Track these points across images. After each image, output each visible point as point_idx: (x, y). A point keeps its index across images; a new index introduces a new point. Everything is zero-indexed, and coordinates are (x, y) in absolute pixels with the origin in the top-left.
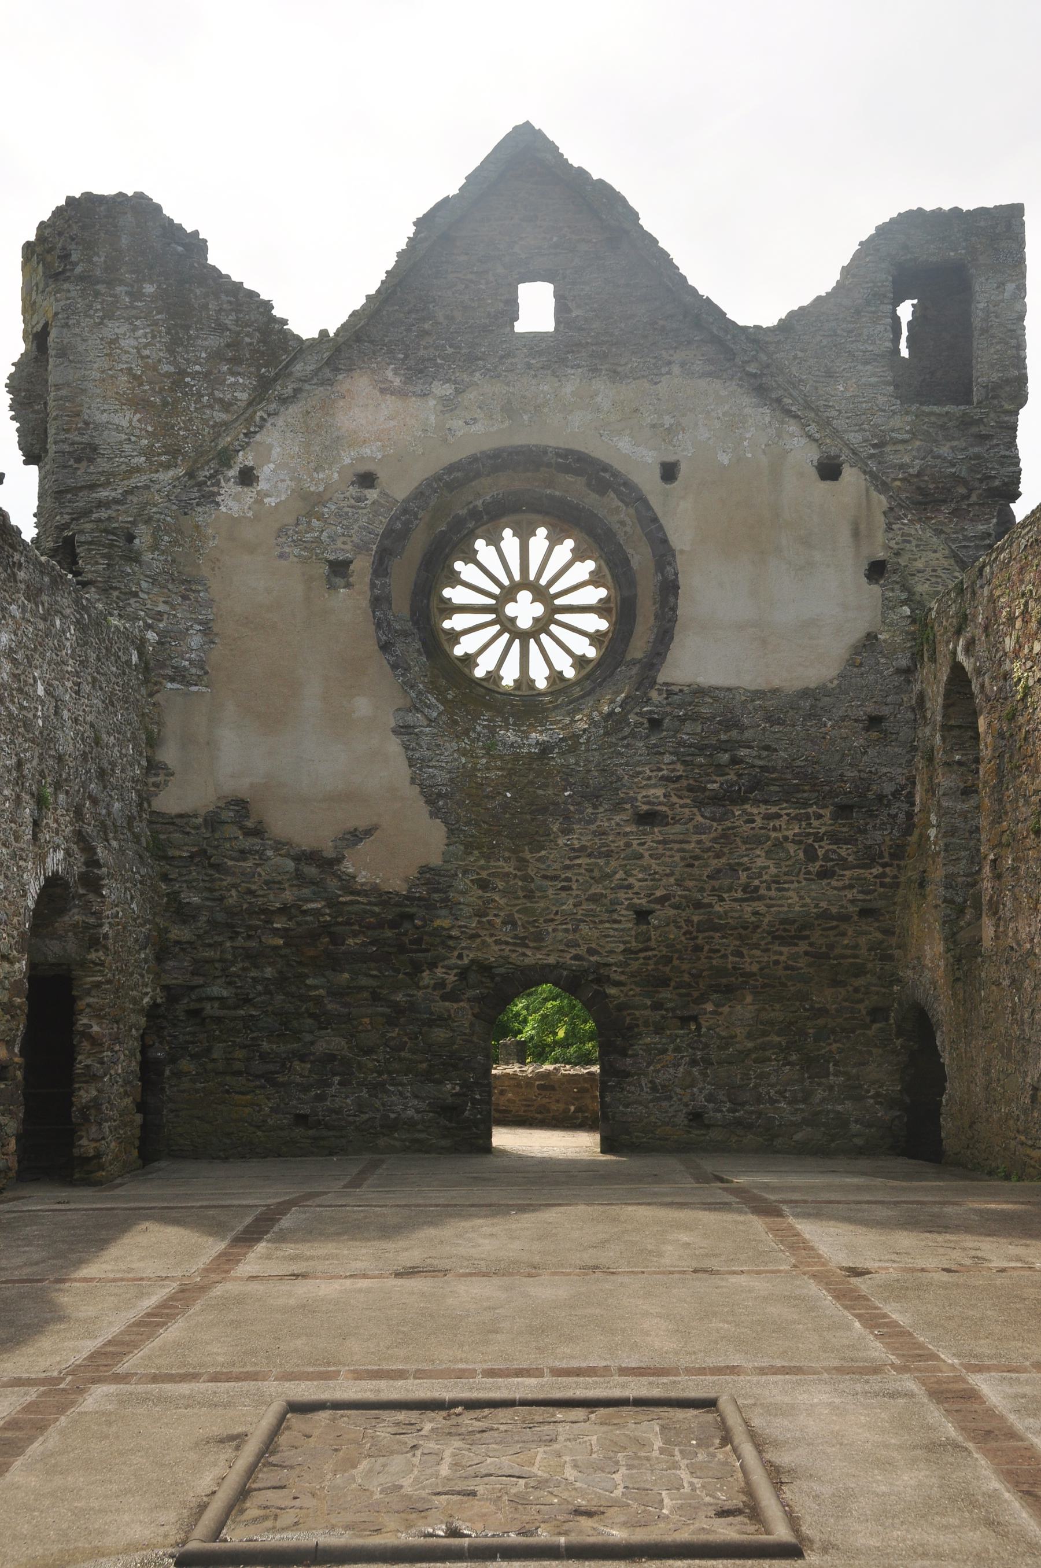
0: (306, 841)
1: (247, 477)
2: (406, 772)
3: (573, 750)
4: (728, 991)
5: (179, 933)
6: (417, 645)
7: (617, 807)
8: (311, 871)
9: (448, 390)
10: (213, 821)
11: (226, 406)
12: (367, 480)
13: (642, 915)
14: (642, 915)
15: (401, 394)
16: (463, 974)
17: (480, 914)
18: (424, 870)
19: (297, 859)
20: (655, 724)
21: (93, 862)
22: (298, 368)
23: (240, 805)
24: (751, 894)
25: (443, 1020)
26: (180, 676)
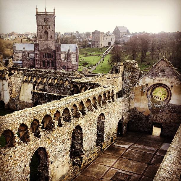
0: (140, 111)
1: (138, 84)
2: (148, 107)
3: (161, 107)
4: (171, 127)
5: (131, 116)
6: (151, 97)
7: (164, 112)
8: (140, 113)
9: (154, 78)
10: (134, 109)
11: (137, 79)
12: (147, 85)
13: (165, 120)
14: (165, 120)
15: (151, 78)
16: (151, 122)
17: (153, 118)
18: (149, 114)
19: (140, 112)
20: (168, 106)
21: (123, 117)
22: (142, 76)
23: (136, 108)
24: (174, 120)
25: (149, 125)
26: (132, 99)
